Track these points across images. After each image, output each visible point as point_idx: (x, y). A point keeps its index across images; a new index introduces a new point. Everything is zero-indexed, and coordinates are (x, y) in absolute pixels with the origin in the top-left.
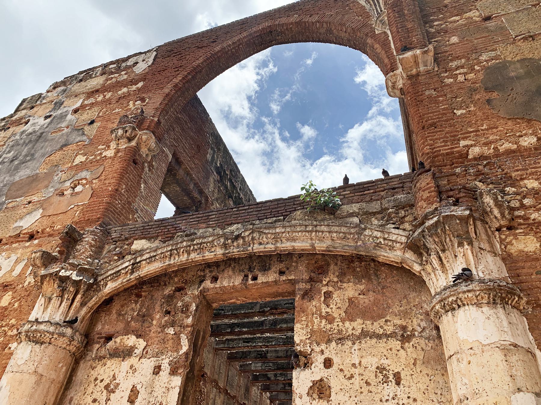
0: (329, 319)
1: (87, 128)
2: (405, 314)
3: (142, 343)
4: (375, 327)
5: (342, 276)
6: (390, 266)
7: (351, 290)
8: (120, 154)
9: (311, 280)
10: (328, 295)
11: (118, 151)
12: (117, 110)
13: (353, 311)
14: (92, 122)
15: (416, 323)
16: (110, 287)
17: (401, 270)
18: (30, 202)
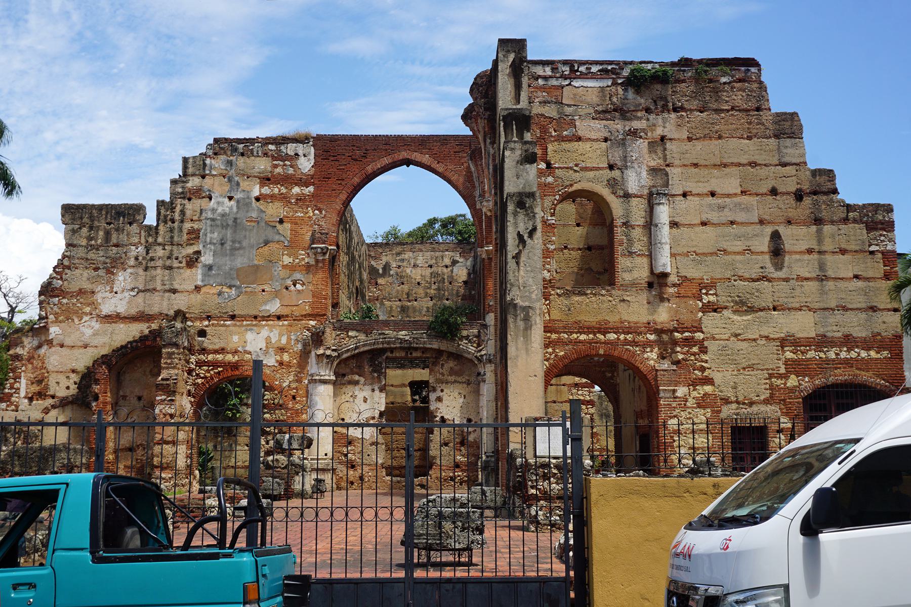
0: (443, 375)
1: (279, 226)
2: (470, 375)
3: (362, 380)
4: (459, 379)
5: (448, 357)
6: (467, 358)
7: (451, 364)
8: (320, 265)
9: (436, 358)
10: (443, 365)
11: (317, 261)
12: (299, 214)
13: (452, 372)
14: (281, 221)
15: (473, 379)
16: (345, 356)
17: (471, 361)
18: (263, 291)
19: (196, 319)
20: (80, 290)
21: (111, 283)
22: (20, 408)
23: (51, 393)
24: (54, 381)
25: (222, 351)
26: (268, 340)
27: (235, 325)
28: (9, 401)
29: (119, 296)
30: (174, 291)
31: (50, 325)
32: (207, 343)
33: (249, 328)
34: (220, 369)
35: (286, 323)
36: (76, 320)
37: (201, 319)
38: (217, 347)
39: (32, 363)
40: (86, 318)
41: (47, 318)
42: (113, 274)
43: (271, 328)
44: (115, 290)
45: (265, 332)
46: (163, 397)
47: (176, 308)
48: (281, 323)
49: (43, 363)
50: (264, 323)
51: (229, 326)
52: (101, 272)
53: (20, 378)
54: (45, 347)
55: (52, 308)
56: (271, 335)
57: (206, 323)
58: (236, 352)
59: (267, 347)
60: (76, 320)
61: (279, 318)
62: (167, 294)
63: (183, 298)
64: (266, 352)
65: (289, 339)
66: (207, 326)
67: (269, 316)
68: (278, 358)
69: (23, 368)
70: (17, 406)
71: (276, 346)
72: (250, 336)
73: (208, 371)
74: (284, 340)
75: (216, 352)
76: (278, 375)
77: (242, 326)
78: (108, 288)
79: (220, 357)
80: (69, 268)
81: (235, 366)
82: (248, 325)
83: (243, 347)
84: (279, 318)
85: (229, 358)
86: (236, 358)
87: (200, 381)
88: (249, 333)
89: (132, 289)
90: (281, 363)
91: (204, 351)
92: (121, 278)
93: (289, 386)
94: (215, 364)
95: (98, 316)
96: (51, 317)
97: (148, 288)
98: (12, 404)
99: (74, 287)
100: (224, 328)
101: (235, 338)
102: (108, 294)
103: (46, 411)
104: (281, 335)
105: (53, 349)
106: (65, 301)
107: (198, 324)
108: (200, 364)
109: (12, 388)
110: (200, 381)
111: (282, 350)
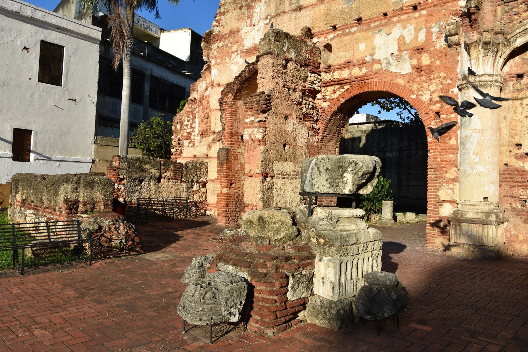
19: (321, 33)
20: (231, 31)
21: (250, 17)
22: (196, 144)
23: (213, 129)
24: (214, 118)
25: (348, 64)
26: (401, 40)
27: (361, 30)
28: (190, 138)
29: (256, 27)
30: (300, 8)
31: (212, 67)
32: (334, 59)
33: (379, 29)
34: (346, 87)
35: (424, 12)
36: (227, 59)
37: (328, 32)
38: (342, 61)
39: (202, 104)
40: (234, 56)
41: (210, 62)
42: (252, 8)
43: (404, 24)
44: (253, 24)
45: (397, 31)
46: (252, 118)
47: (302, 26)
48: (417, 14)
49: (208, 103)
50: (395, 19)
51: (355, 32)
52: (244, 10)
53: (195, 119)
54: (210, 88)
55: (213, 53)
56: (405, 33)
57: (331, 36)
58: (363, 63)
59: (400, 50)
60: (227, 59)
61: (415, 8)
62: (294, 15)
63: (308, 13)
64: (399, 58)
65: (429, 33)
66: (330, 40)
67: (402, 9)
68: (415, 62)
69: (197, 110)
70: (194, 143)
71: (411, 47)
72: (379, 39)
73: (334, 92)
74: (422, 36)
75: (341, 67)
76: (415, 87)
77: (369, 29)
78: (249, 22)
79: (345, 74)
80: (223, 14)
81: (361, 80)
82: (376, 27)
83: (371, 55)
84: (415, 8)
85: (357, 72)
86: (364, 70)
87: (325, 105)
88: (377, 36)
89: (266, 18)
90: (419, 69)
91: (329, 68)
92: (257, 10)
93: (431, 100)
94: (341, 83)
95: (242, 52)
96: (213, 61)
97: (278, 12)
98: (192, 141)
99: (225, 30)
100: (348, 38)
101: (362, 47)
102: (249, 29)
103: (210, 147)
104: (417, 30)
105: (213, 90)
106: (221, 44)
107: (322, 39)
108: (326, 85)
109: (191, 127)
110: (325, 105)
111: (419, 50)
